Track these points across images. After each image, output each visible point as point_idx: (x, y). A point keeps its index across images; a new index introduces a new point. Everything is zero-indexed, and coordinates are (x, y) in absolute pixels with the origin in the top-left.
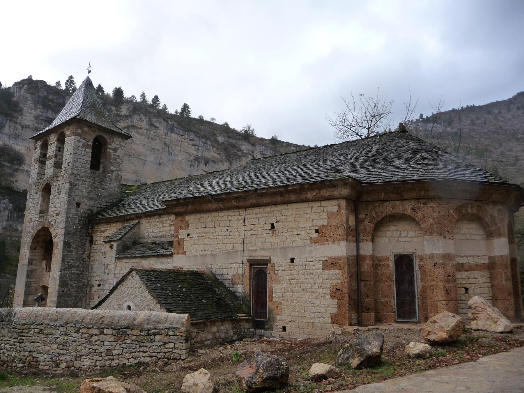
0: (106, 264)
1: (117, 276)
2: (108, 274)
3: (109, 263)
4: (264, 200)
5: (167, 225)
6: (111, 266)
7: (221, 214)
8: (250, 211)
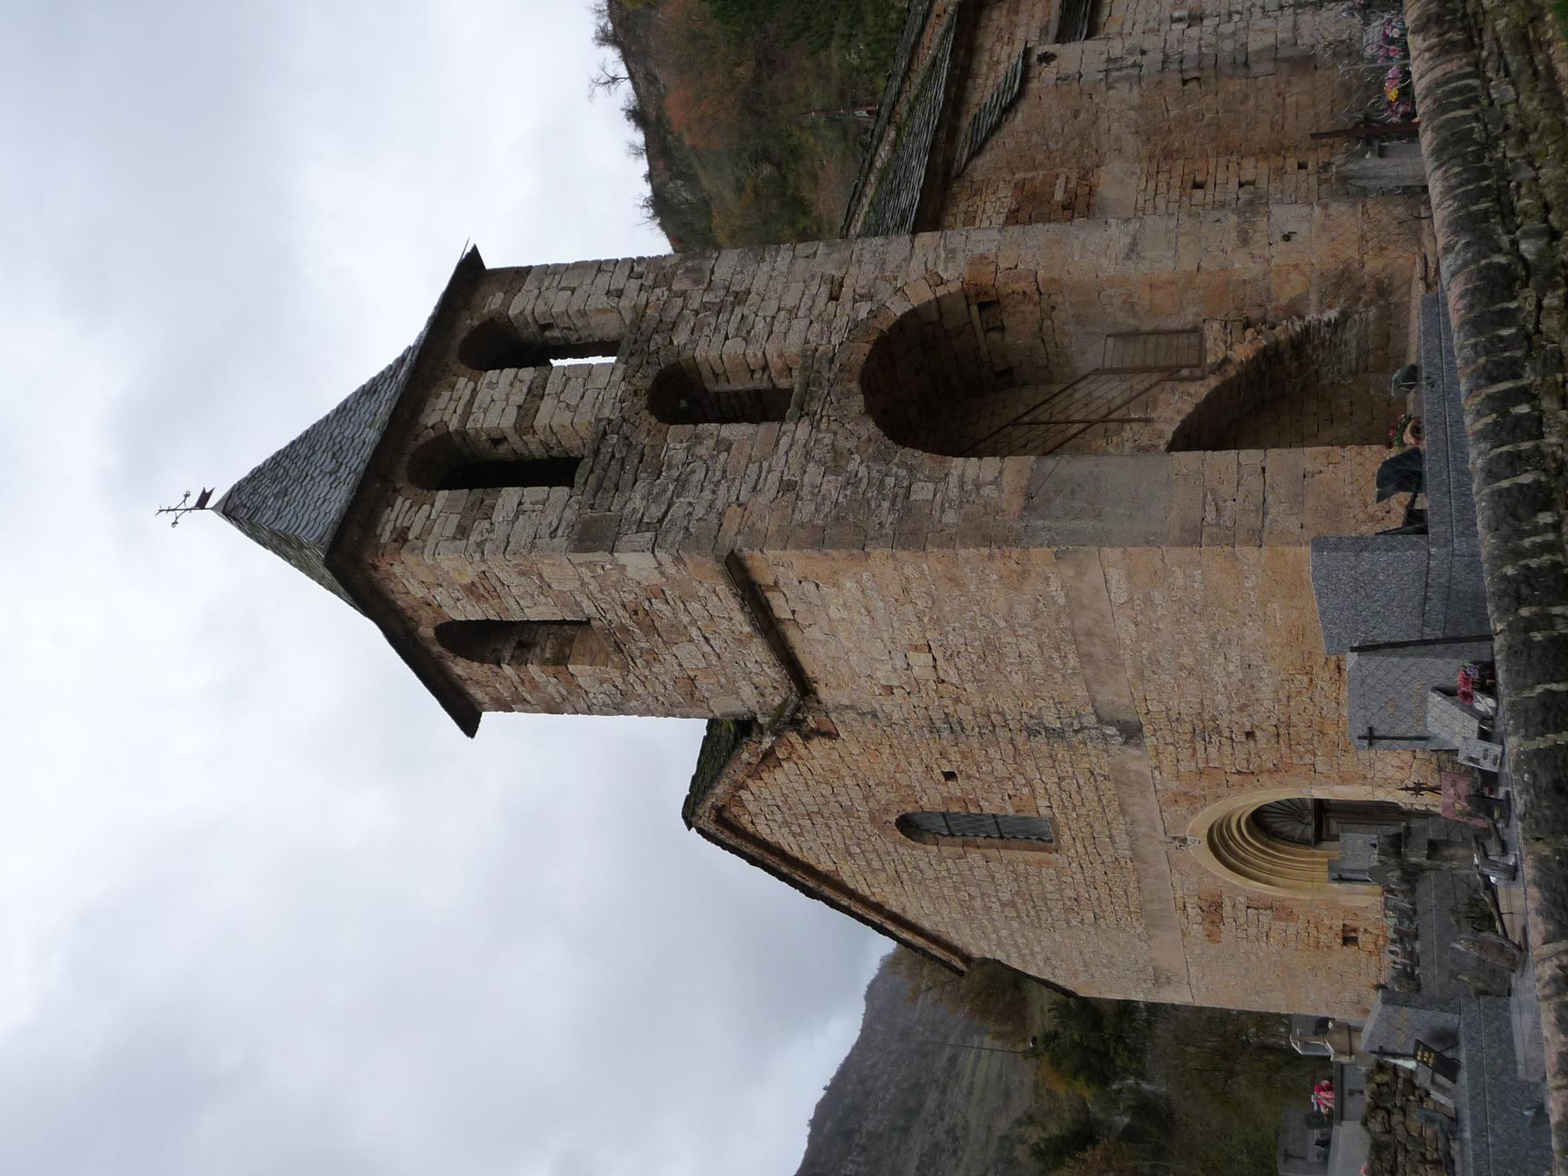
0: (1104, 67)
1: (1152, 24)
2: (1143, 53)
3: (1104, 57)
5: (1007, 49)
6: (1117, 48)
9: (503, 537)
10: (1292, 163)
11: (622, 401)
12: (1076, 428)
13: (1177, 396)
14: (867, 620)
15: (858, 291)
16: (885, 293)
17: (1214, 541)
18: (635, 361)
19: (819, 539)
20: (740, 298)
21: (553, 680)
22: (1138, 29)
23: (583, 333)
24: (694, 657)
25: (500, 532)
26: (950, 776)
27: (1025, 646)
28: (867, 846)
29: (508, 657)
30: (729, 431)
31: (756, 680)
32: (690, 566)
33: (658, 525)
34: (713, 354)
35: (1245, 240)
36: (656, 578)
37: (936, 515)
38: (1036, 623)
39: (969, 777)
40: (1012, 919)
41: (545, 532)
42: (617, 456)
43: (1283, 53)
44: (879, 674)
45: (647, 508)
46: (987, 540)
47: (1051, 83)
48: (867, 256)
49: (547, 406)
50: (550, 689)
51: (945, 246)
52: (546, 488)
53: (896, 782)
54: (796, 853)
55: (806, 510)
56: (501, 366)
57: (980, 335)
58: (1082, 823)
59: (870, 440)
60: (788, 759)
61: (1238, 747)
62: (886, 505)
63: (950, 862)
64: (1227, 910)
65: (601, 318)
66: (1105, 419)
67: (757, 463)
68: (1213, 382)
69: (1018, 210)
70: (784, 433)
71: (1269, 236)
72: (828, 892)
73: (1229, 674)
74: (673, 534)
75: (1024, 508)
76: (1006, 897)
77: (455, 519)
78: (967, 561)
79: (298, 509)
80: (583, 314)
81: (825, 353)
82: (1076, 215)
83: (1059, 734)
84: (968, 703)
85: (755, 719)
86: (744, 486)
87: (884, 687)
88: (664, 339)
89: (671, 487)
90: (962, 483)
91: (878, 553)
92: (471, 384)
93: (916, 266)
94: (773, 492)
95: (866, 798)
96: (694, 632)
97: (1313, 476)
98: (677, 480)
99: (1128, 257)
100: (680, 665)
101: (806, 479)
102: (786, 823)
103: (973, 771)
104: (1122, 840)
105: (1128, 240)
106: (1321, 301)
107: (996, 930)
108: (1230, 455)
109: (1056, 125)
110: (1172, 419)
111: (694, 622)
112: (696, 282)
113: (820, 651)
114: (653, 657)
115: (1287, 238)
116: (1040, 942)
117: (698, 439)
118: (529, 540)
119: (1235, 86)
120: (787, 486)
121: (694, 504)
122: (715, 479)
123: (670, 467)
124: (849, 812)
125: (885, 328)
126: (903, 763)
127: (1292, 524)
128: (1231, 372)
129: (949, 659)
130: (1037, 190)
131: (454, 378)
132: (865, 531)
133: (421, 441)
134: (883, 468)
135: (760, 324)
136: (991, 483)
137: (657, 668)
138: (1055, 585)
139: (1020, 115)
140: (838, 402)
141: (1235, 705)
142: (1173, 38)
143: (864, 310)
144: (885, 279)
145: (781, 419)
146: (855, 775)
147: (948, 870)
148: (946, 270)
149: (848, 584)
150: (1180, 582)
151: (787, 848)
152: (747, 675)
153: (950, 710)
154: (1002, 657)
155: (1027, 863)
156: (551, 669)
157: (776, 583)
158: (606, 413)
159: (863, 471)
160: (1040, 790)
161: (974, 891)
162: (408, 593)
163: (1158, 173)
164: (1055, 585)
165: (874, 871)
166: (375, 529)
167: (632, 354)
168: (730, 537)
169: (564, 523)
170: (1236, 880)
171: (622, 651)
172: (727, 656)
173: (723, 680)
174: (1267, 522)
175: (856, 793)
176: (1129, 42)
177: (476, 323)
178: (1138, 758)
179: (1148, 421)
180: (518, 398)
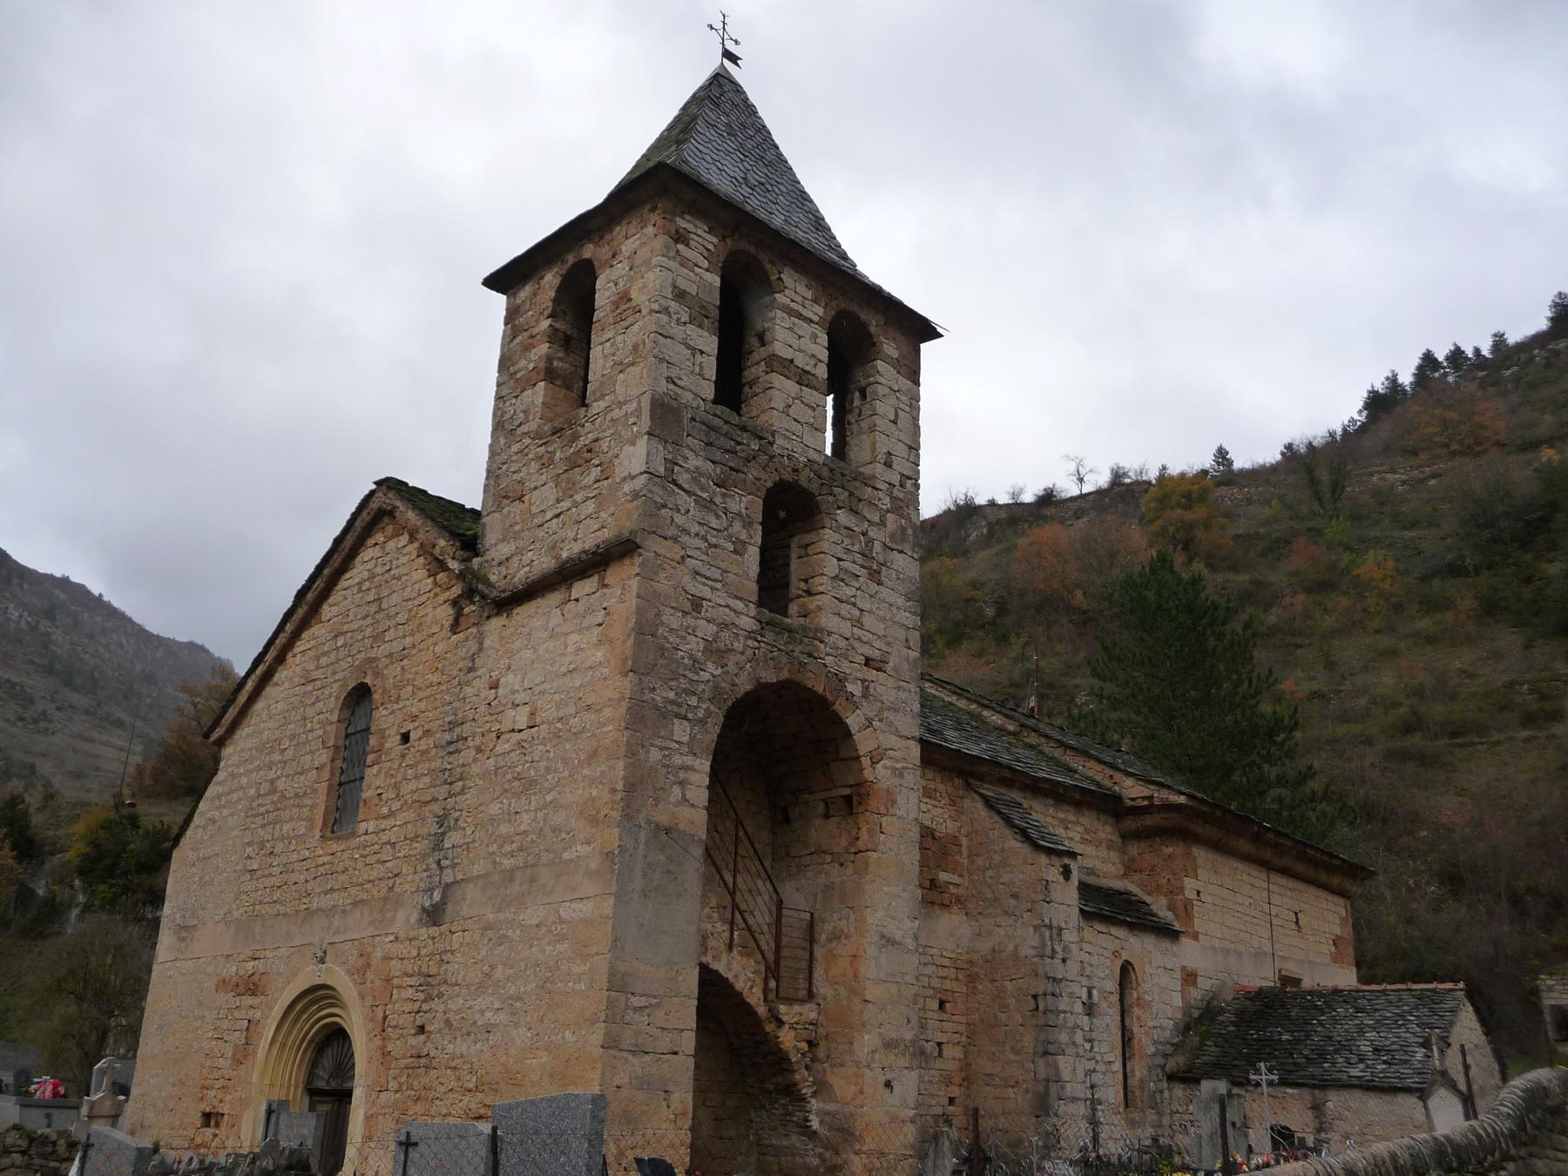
0: (1055, 924)
1: (1088, 970)
2: (1064, 960)
3: (1063, 925)
4: (1299, 867)
5: (1077, 839)
6: (1070, 936)
7: (1241, 866)
8: (1275, 877)
9: (671, 332)
10: (955, 1091)
11: (789, 457)
12: (729, 878)
13: (750, 975)
14: (564, 669)
15: (872, 685)
16: (868, 709)
17: (611, 1003)
18: (825, 473)
19: (645, 630)
20: (875, 575)
21: (531, 366)
23: (854, 427)
24: (542, 502)
25: (678, 331)
26: (405, 738)
27: (525, 821)
28: (343, 653)
29: (557, 325)
30: (753, 554)
31: (515, 559)
32: (630, 506)
33: (670, 479)
34: (825, 546)
35: (889, 1045)
36: (620, 473)
37: (658, 742)
38: (547, 830)
39: (403, 756)
40: (258, 790)
41: (674, 373)
42: (739, 448)
43: (1053, 1088)
44: (510, 677)
45: (687, 470)
46: (631, 788)
47: (1044, 876)
48: (903, 695)
49: (791, 386)
50: (523, 363)
51: (907, 768)
52: (714, 378)
53: (404, 686)
54: (343, 583)
55: (673, 619)
56: (832, 347)
58: (348, 863)
59: (733, 685)
60: (436, 584)
61: (410, 1018)
62: (672, 695)
63: (320, 732)
64: (248, 1000)
65: (867, 445)
66: (735, 906)
67: (720, 578)
68: (762, 1010)
69: (934, 838)
70: (747, 606)
71: (890, 1067)
72: (300, 612)
73: (482, 1012)
74: (661, 492)
75: (657, 825)
76: (280, 785)
77: (693, 290)
78: (612, 768)
79: (714, 143)
80: (873, 428)
81: (817, 650)
82: (925, 891)
83: (438, 845)
84: (475, 760)
85: (477, 555)
86: (700, 564)
87: (498, 681)
88: (843, 501)
89: (705, 495)
91: (626, 685)
92: (816, 319)
93: (891, 740)
95: (390, 655)
96: (565, 504)
97: (665, 1099)
98: (711, 501)
99: (883, 936)
100: (535, 488)
101: (702, 623)
102: (373, 576)
103: (409, 760)
104: (327, 901)
105: (898, 937)
106: (828, 1113)
107: (245, 774)
108: (692, 1023)
109: (1006, 878)
110: (730, 970)
111: (576, 505)
112: (892, 536)
113: (537, 623)
114: (546, 463)
115: (888, 1084)
116: (232, 815)
117: (748, 524)
118: (667, 357)
119: (1028, 1042)
120: (697, 604)
121: (689, 516)
122: (709, 537)
123: (724, 495)
124: (378, 638)
126: (421, 694)
127: (622, 1078)
128: (769, 1028)
129: (519, 744)
130: (950, 857)
131: (823, 304)
132: (648, 674)
133: (768, 266)
134: (706, 696)
135: (849, 592)
136: (684, 796)
137: (534, 466)
138: (582, 850)
139: (1018, 845)
140: (771, 659)
141: (451, 1016)
142: (1075, 988)
143: (854, 688)
144: (881, 710)
145: (760, 604)
146: (414, 646)
147: (312, 730)
148: (885, 767)
149: (599, 654)
150: (576, 970)
151: (347, 575)
152: (520, 551)
153: (470, 743)
154: (517, 795)
155: (312, 807)
156: (542, 365)
157: (605, 586)
158: (779, 441)
159: (705, 676)
160: (384, 824)
161: (289, 754)
162: (627, 238)
163: (957, 968)
164: (582, 850)
165: (317, 658)
166: (689, 213)
167: (832, 470)
168: (653, 545)
169: (679, 391)
170: (278, 1011)
171: (553, 434)
172: (541, 533)
173: (517, 528)
174: (625, 1054)
175: (396, 646)
176: (1074, 947)
177: (873, 329)
178: (408, 921)
179: (730, 946)
180: (800, 361)
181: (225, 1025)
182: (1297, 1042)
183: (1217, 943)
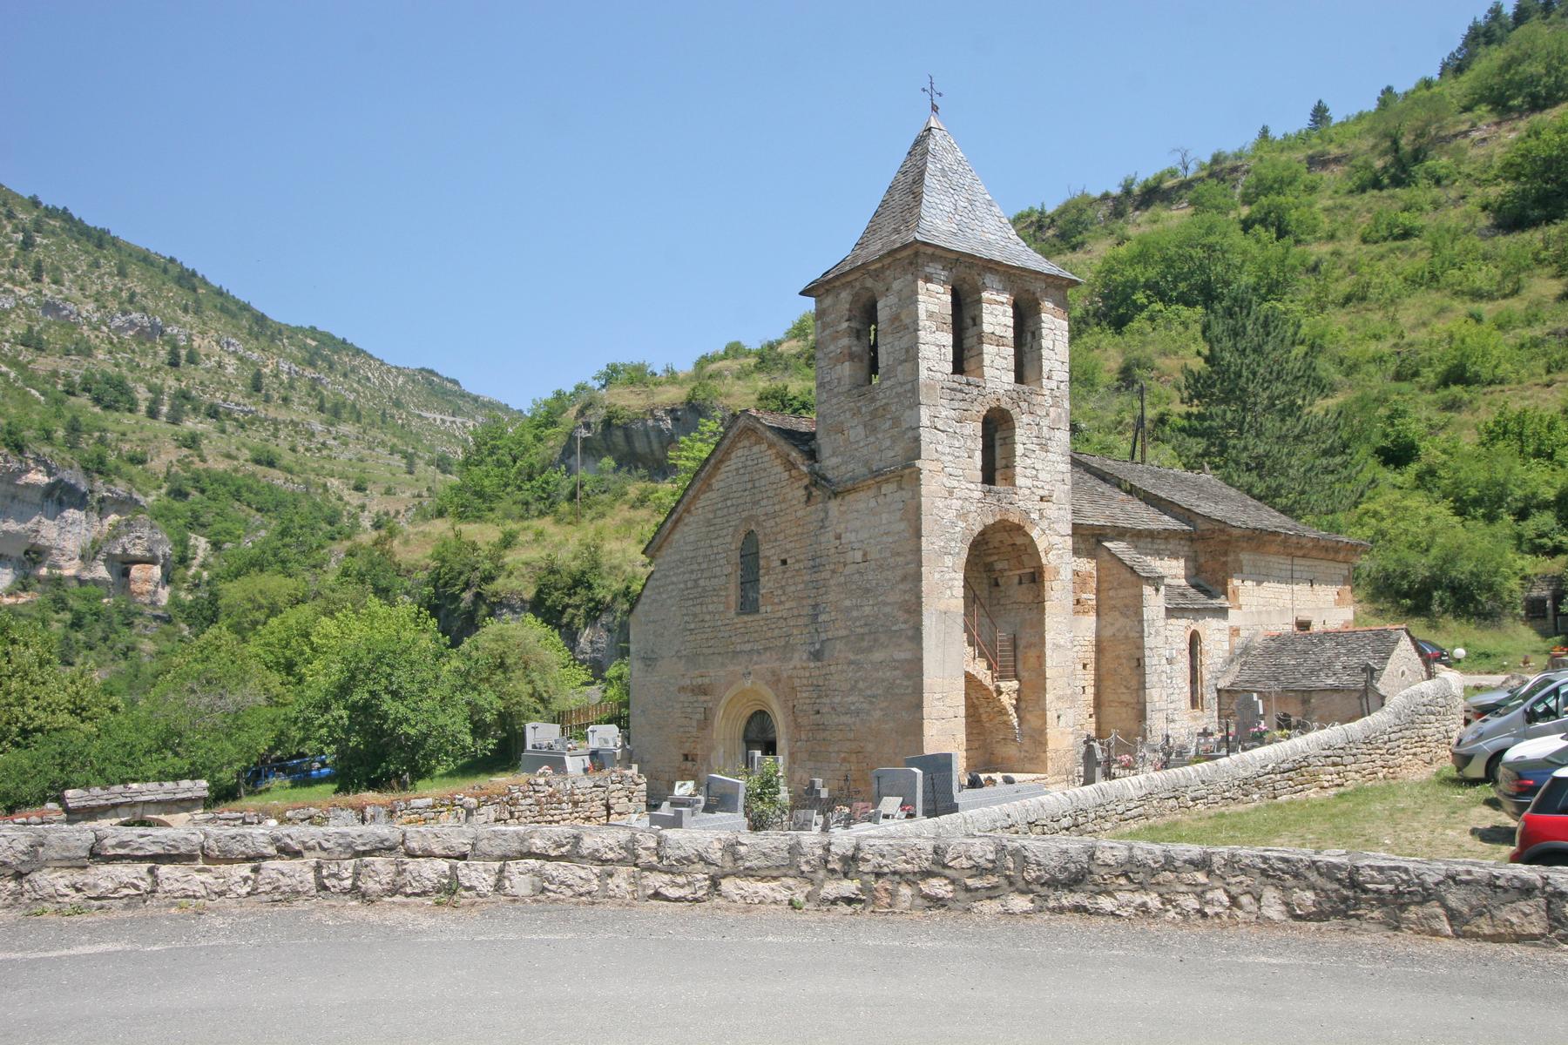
16: (1044, 524)
22: (1168, 633)
48: (1062, 512)
55: (940, 503)
57: (1018, 572)
60: (791, 476)
64: (702, 698)
90: (951, 579)
94: (948, 485)
125: (1026, 528)
142: (1162, 651)
143: (1035, 516)
145: (983, 482)
157: (902, 489)
160: (776, 608)
176: (1162, 629)
181: (689, 710)
182: (1300, 664)
183: (1254, 609)
